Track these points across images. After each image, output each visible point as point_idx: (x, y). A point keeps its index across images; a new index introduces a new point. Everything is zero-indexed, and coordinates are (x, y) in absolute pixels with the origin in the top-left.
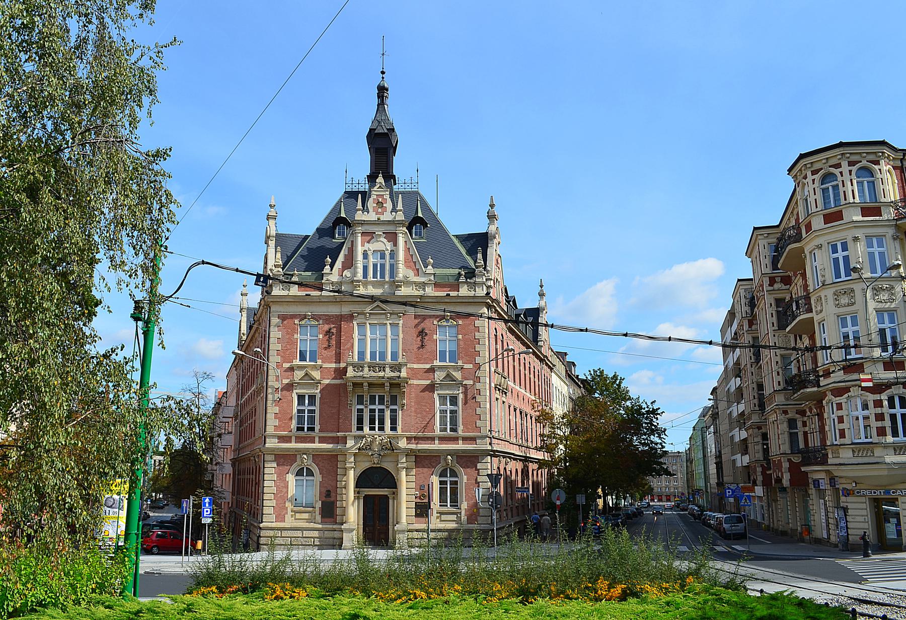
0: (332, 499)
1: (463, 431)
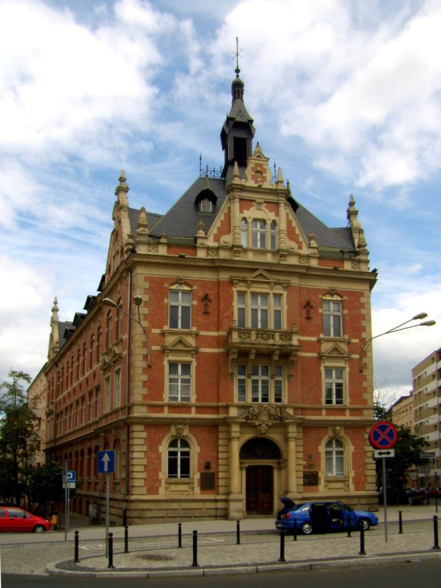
0: (212, 471)
1: (350, 403)
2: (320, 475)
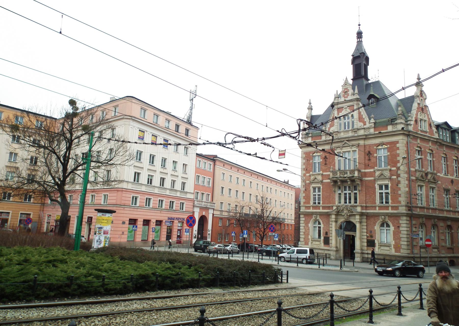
0: (328, 236)
1: (392, 203)
2: (376, 242)
